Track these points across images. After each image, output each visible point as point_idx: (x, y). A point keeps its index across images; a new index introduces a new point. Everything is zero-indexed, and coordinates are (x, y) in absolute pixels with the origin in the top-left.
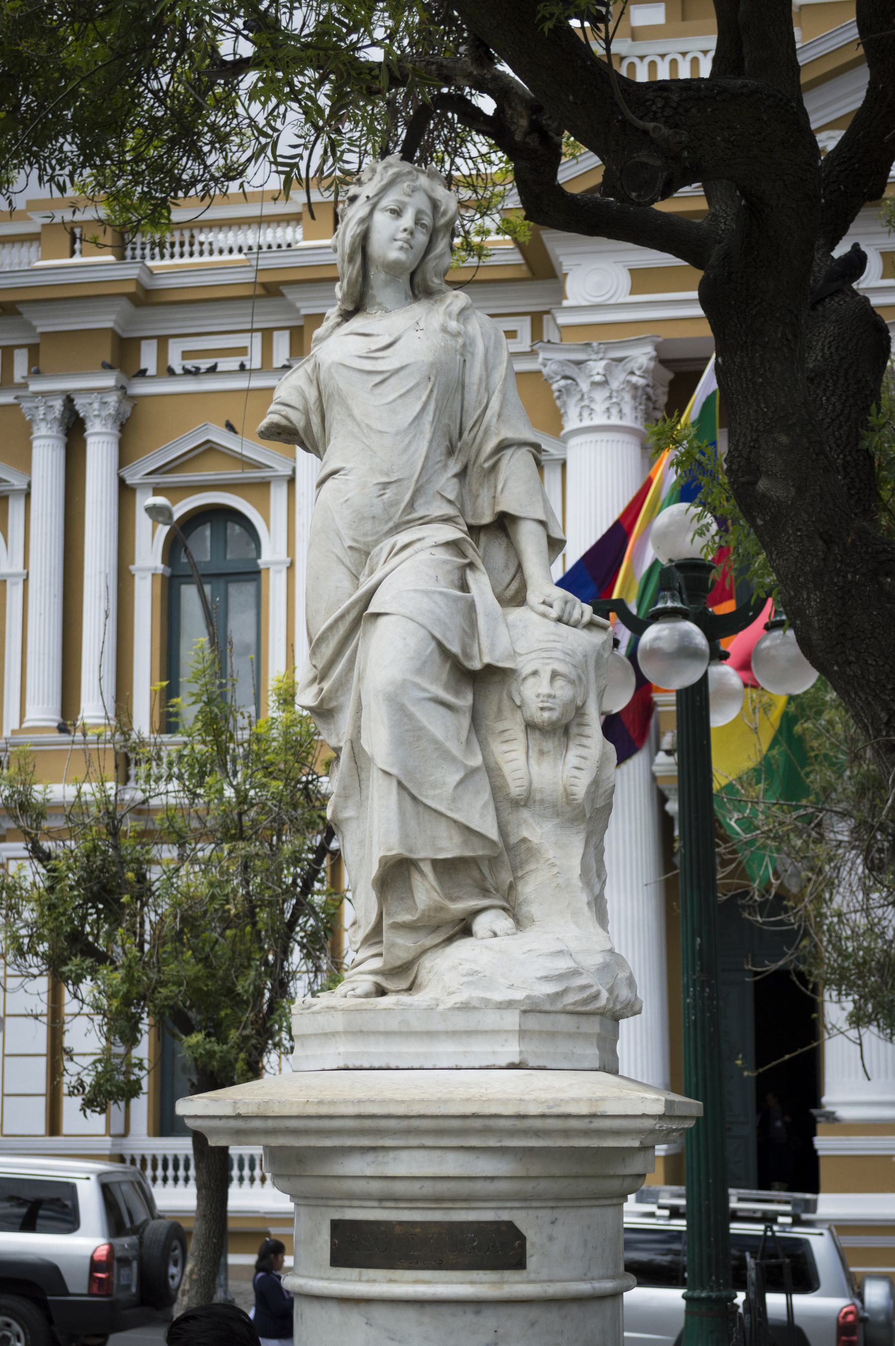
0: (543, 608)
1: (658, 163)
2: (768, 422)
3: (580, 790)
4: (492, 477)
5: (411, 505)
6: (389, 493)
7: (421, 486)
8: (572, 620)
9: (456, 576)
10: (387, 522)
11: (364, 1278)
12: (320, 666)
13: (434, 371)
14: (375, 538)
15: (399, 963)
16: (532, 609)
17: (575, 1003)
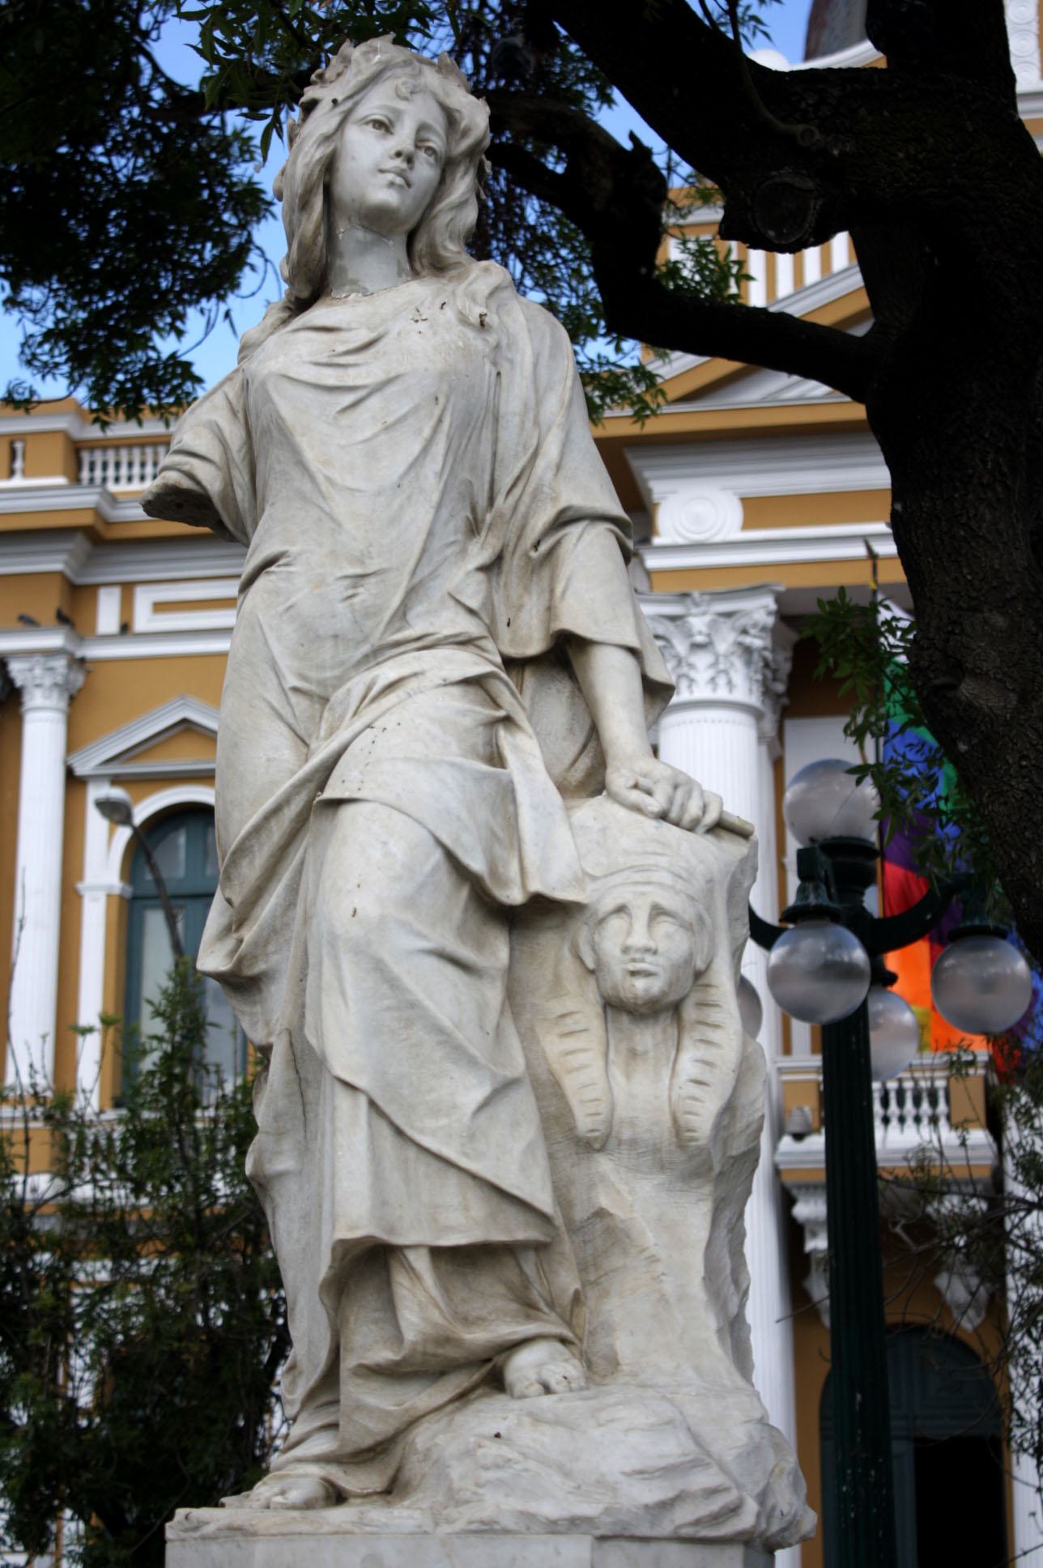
0: (636, 796)
1: (811, 184)
2: (974, 594)
3: (703, 1119)
4: (546, 573)
5: (402, 614)
6: (366, 594)
7: (421, 583)
8: (687, 819)
9: (479, 738)
10: (358, 643)
12: (237, 900)
13: (445, 387)
14: (337, 672)
15: (368, 1442)
16: (614, 798)
17: (697, 1522)
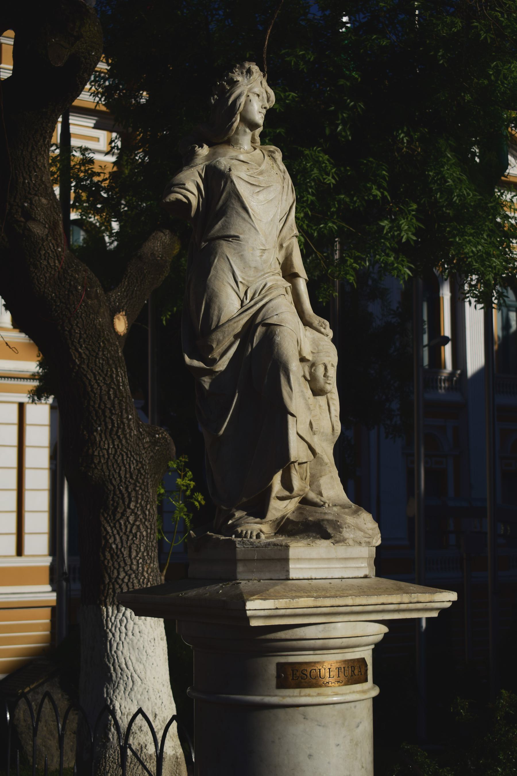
11: (302, 694)
